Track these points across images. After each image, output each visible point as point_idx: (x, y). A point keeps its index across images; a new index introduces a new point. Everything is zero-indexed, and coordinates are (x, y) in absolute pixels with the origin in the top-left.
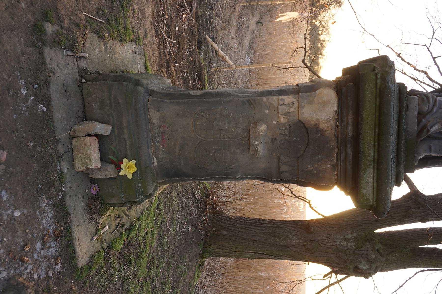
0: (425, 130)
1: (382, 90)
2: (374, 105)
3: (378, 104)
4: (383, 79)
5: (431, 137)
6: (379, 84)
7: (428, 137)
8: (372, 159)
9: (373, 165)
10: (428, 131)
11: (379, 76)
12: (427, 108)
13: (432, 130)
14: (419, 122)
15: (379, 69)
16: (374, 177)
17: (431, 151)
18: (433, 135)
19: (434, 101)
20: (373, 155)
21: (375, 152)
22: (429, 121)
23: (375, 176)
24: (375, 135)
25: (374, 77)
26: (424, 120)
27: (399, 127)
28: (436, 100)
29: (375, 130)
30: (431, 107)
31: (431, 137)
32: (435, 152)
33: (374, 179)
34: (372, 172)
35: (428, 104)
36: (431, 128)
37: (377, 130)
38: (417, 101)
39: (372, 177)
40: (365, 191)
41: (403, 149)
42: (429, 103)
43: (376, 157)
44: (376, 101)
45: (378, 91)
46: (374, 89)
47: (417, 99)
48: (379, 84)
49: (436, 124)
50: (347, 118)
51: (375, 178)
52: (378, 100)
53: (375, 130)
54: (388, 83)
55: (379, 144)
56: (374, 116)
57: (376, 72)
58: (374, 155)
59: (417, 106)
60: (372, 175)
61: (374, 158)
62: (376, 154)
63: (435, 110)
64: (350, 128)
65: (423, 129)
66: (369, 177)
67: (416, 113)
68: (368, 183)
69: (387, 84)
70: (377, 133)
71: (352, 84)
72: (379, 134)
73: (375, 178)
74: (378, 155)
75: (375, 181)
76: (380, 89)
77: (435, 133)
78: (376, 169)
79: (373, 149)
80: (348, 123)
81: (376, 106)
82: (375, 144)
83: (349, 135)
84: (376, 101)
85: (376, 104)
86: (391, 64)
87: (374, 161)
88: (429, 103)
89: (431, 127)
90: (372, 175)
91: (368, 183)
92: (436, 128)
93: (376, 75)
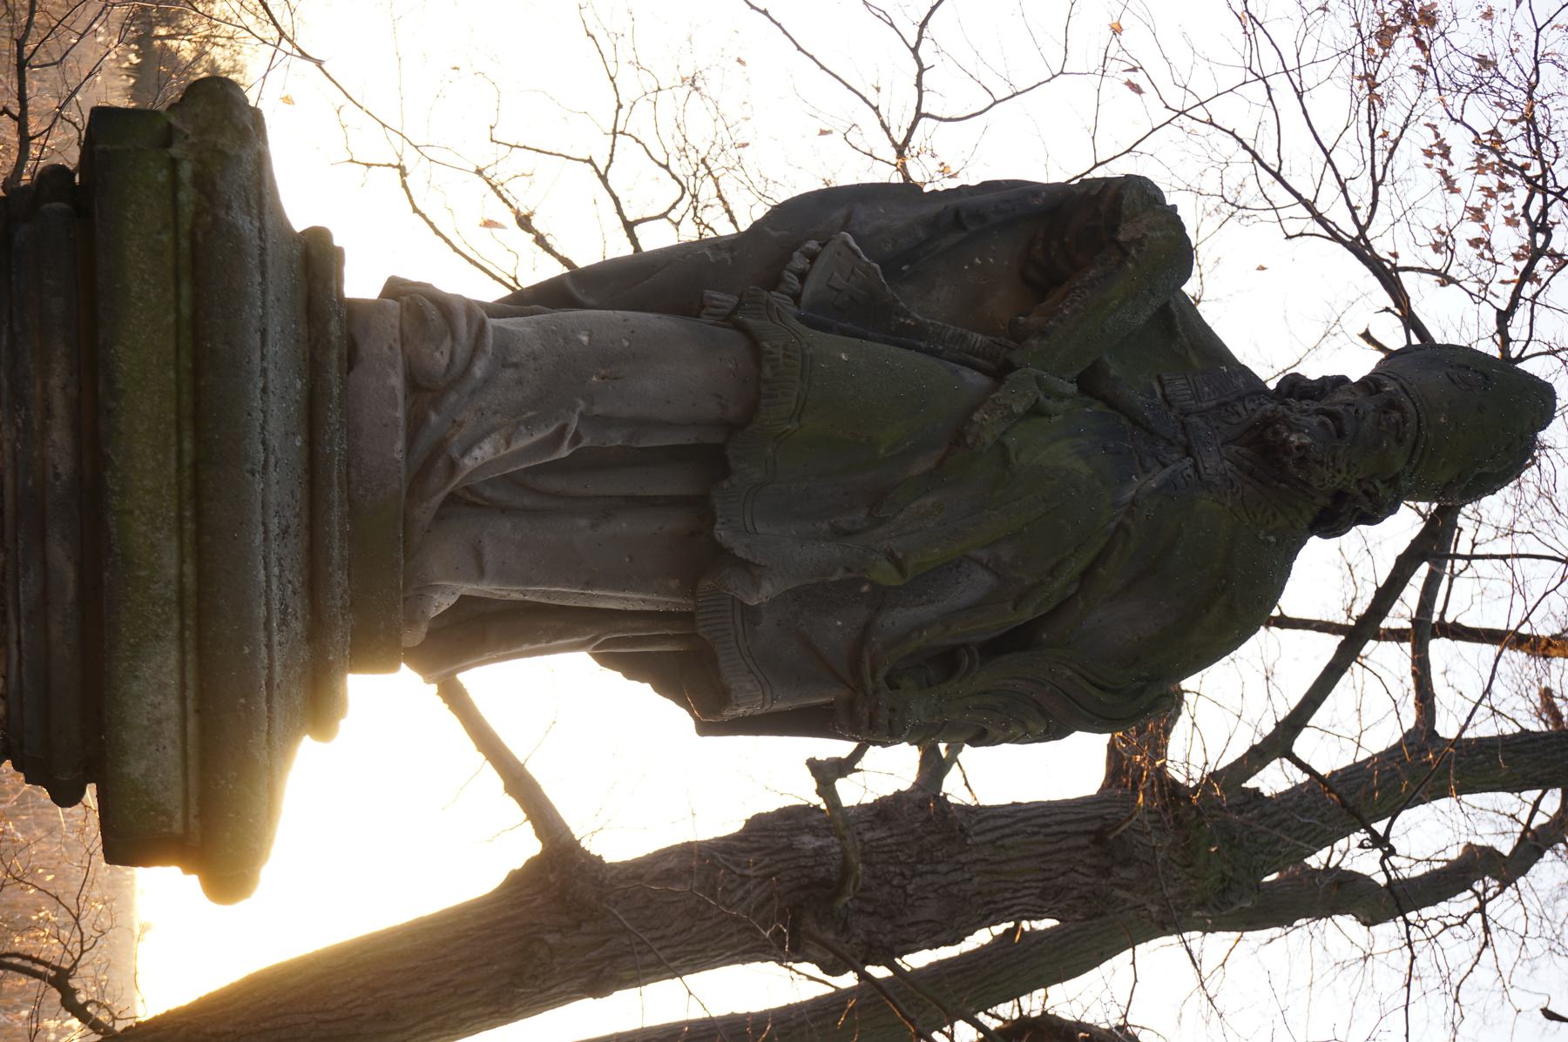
0: (440, 463)
1: (200, 239)
2: (171, 318)
3: (186, 310)
4: (206, 185)
5: (464, 502)
6: (188, 210)
7: (452, 499)
8: (171, 593)
9: (176, 625)
10: (453, 467)
11: (186, 171)
12: (444, 361)
13: (469, 463)
14: (415, 424)
15: (192, 139)
16: (183, 685)
17: (481, 574)
18: (488, 493)
19: (475, 328)
20: (173, 572)
21: (182, 561)
22: (460, 425)
23: (191, 683)
24: (179, 470)
25: (162, 176)
26: (434, 418)
27: (312, 443)
28: (483, 324)
29: (180, 443)
30: (462, 354)
31: (464, 502)
32: (504, 576)
33: (183, 699)
34: (173, 661)
35: (448, 343)
36: (463, 456)
37: (188, 445)
38: (397, 323)
39: (173, 691)
40: (144, 764)
41: (336, 553)
42: (454, 339)
43: (190, 580)
44: (178, 295)
45: (185, 243)
46: (165, 238)
47: (397, 312)
48: (188, 210)
49: (487, 434)
50: (45, 385)
51: (191, 694)
52: (186, 290)
53: (180, 443)
54: (229, 207)
55: (198, 513)
56: (172, 374)
57: (176, 151)
58: (181, 575)
59: (398, 346)
60: (173, 681)
61: (181, 590)
62: (189, 569)
63: (478, 371)
64: (60, 435)
65: (430, 460)
66: (162, 687)
67: (397, 381)
68: (159, 722)
69: (222, 213)
70: (188, 460)
71: (64, 205)
72: (196, 465)
73: (191, 694)
74: (200, 574)
75: (191, 706)
76: (192, 235)
77: (490, 483)
78: (190, 645)
79: (174, 544)
80: (48, 412)
81: (177, 321)
82: (180, 518)
83: (57, 476)
84: (178, 295)
85: (178, 311)
86: (247, 119)
87: (181, 603)
88: (454, 339)
89: (466, 451)
90: (176, 676)
91: (159, 722)
92: (484, 451)
93: (174, 163)
